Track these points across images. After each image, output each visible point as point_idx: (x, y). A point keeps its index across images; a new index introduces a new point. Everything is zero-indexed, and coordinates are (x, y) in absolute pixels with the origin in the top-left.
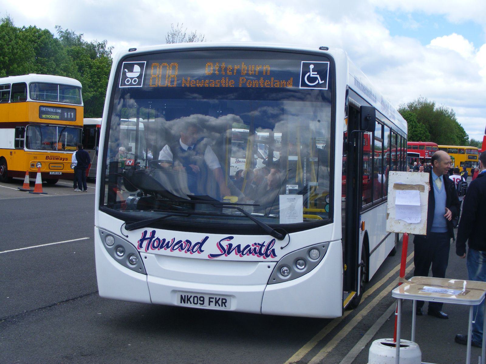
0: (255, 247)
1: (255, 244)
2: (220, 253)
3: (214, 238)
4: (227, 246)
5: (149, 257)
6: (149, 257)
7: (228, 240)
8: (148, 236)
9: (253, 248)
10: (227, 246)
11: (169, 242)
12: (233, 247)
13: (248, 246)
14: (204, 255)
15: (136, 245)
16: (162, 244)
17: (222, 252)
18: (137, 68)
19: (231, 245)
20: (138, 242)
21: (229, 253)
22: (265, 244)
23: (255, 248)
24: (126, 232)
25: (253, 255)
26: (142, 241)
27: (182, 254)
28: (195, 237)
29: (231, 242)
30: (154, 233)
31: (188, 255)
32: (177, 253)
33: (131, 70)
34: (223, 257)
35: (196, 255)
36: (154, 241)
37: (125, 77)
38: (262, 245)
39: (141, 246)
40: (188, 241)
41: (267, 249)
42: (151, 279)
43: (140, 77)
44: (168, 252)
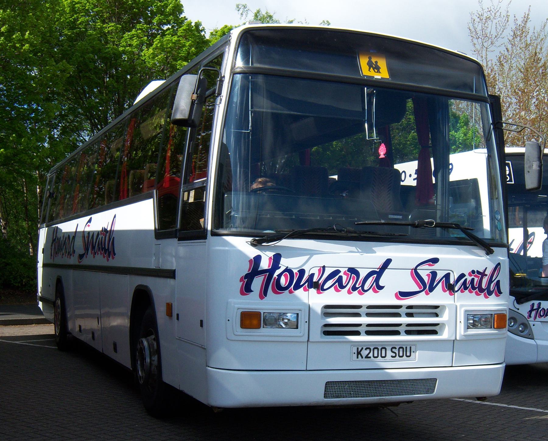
0: (473, 277)
1: (473, 272)
2: (418, 290)
4: (428, 275)
7: (430, 265)
9: (469, 278)
10: (428, 275)
11: (312, 275)
12: (439, 277)
13: (462, 276)
17: (420, 287)
19: (434, 274)
20: (241, 280)
21: (432, 289)
22: (488, 272)
23: (473, 279)
25: (470, 292)
29: (436, 267)
36: (280, 276)
38: (483, 274)
40: (353, 271)
41: (490, 281)
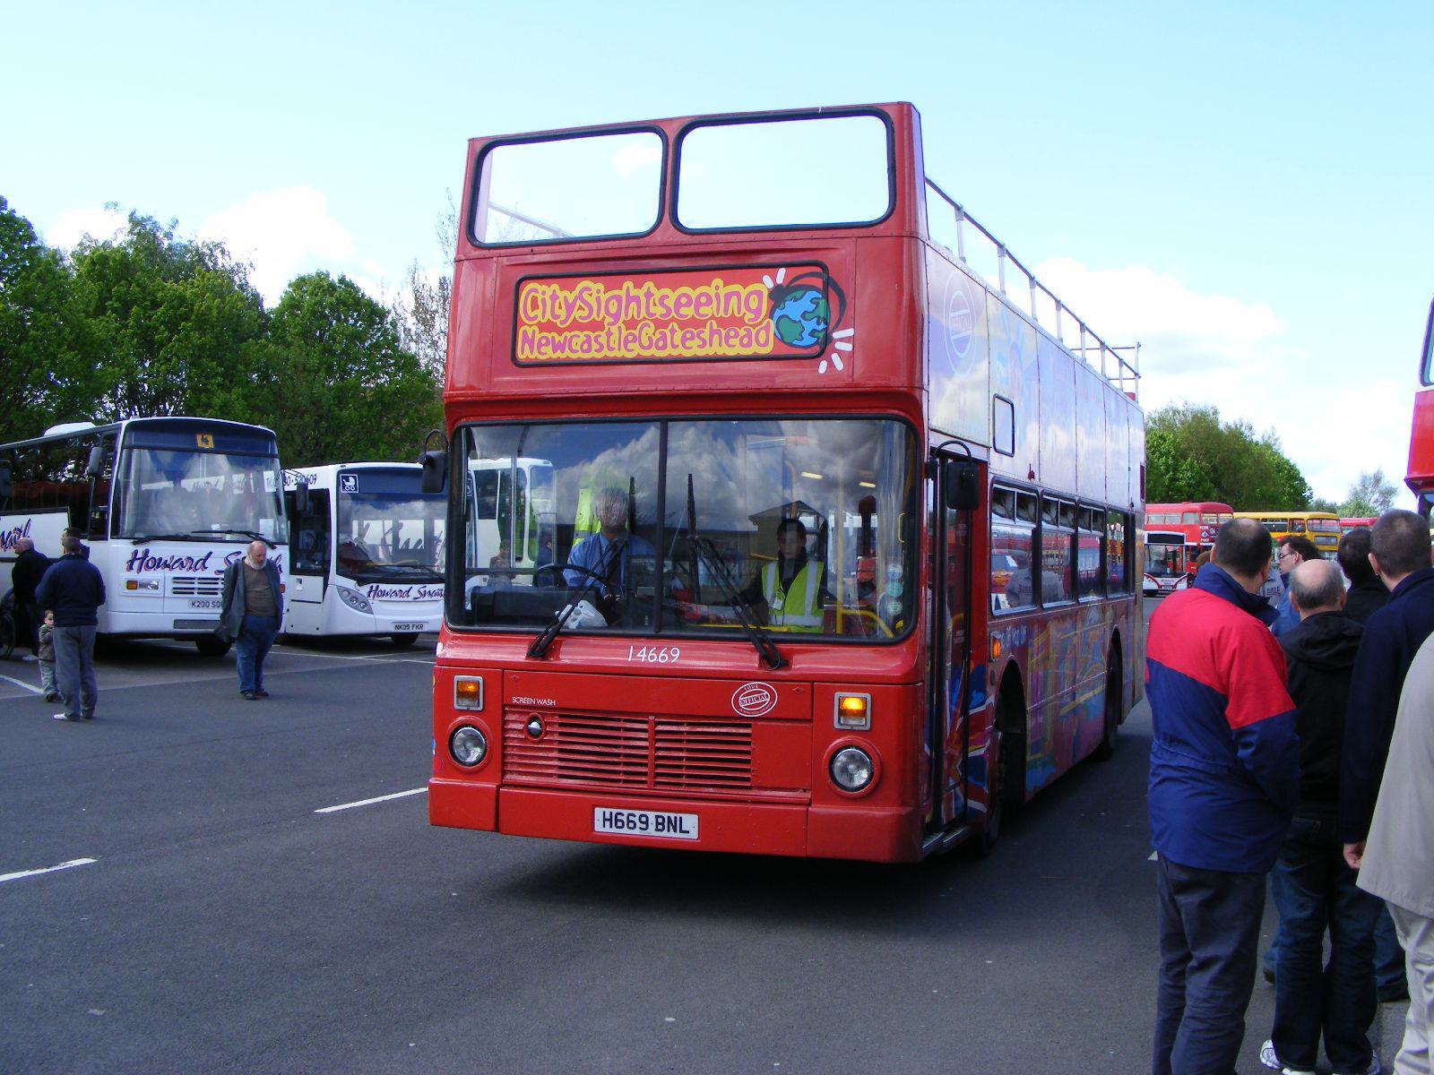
3: (416, 587)
5: (375, 603)
6: (375, 603)
8: (374, 589)
14: (410, 599)
15: (366, 595)
16: (384, 593)
18: (351, 479)
24: (358, 588)
26: (370, 592)
27: (398, 599)
28: (405, 587)
30: (378, 586)
31: (401, 599)
32: (394, 598)
33: (348, 481)
34: (421, 599)
35: (406, 599)
37: (344, 486)
39: (369, 596)
42: (377, 616)
43: (355, 485)
44: (388, 598)
